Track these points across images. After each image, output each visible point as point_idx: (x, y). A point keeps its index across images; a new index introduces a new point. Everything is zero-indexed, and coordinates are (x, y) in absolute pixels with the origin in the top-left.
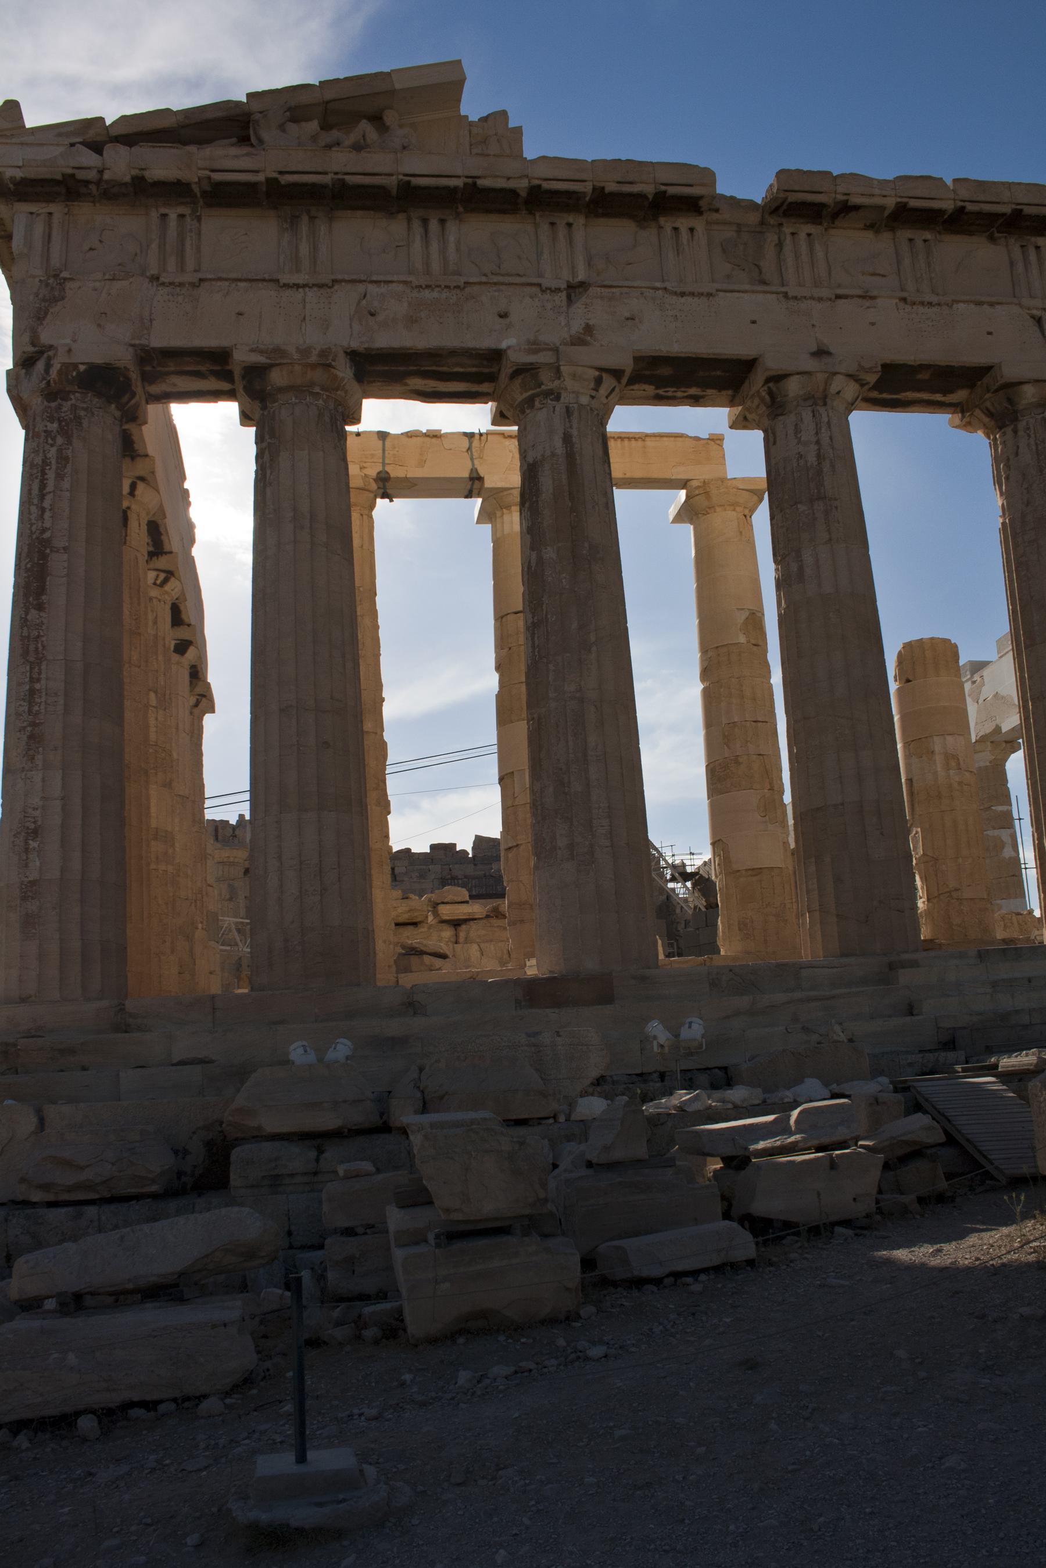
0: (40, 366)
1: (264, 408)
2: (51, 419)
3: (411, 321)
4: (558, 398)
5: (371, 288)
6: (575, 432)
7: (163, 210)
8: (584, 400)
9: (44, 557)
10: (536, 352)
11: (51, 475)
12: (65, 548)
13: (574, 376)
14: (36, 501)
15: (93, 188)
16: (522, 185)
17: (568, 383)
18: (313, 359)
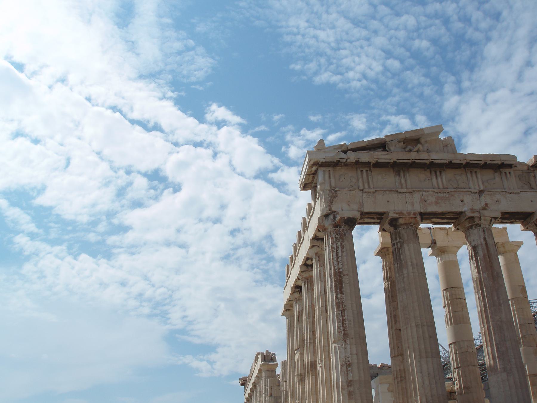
0: (331, 217)
1: (395, 229)
2: (337, 234)
3: (437, 203)
4: (480, 226)
5: (424, 193)
6: (486, 237)
7: (362, 169)
8: (487, 226)
9: (340, 277)
10: (473, 212)
11: (339, 251)
12: (347, 274)
13: (485, 220)
14: (335, 259)
15: (343, 164)
16: (465, 162)
17: (483, 222)
18: (412, 216)
